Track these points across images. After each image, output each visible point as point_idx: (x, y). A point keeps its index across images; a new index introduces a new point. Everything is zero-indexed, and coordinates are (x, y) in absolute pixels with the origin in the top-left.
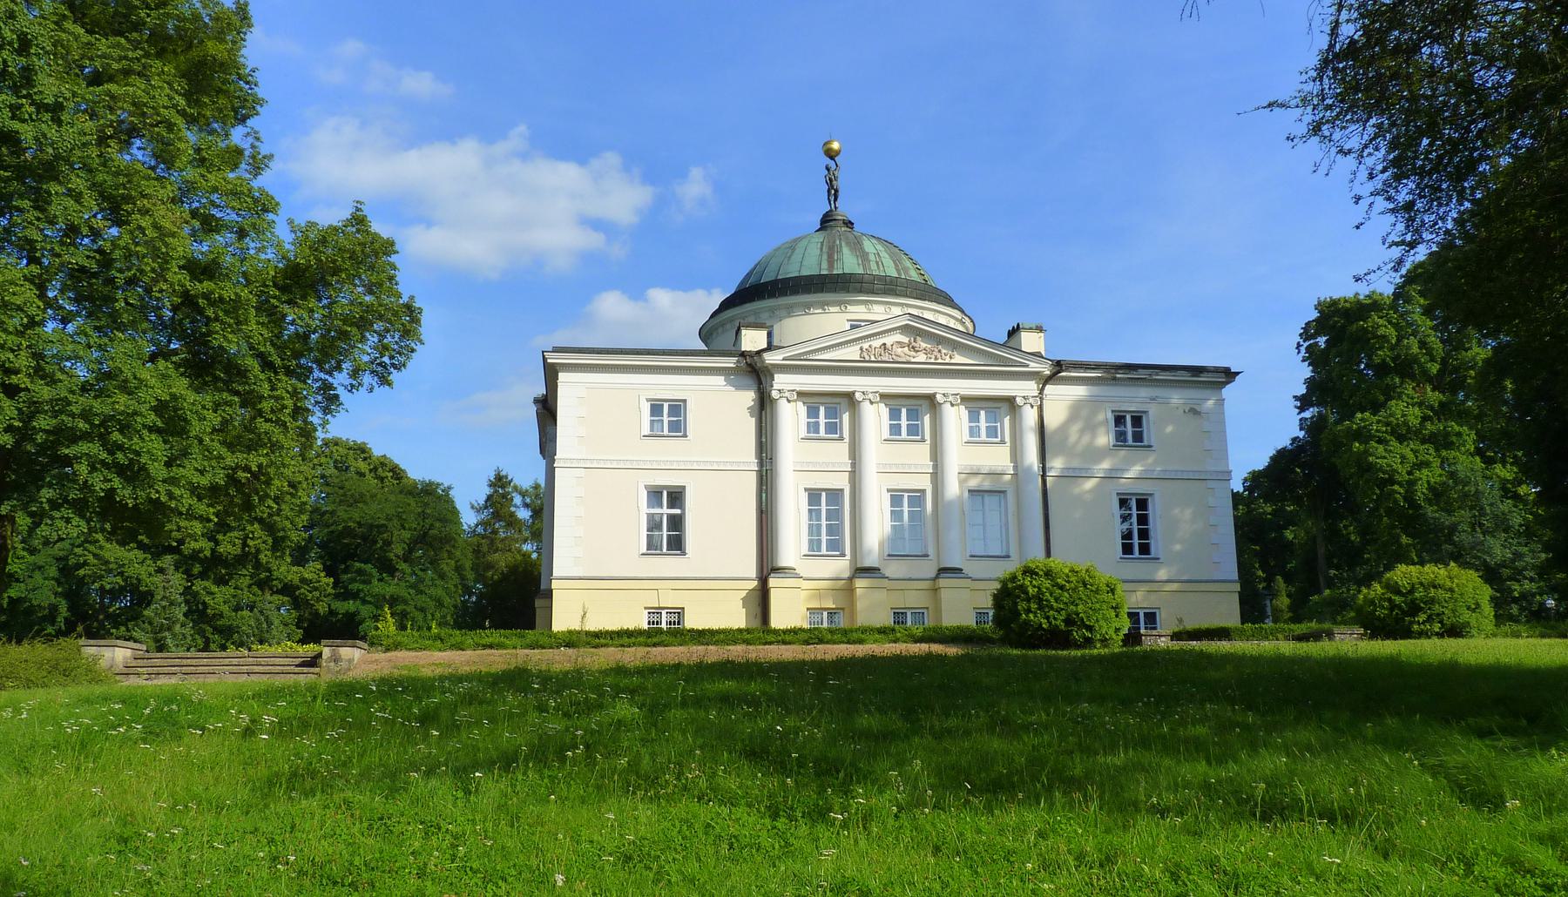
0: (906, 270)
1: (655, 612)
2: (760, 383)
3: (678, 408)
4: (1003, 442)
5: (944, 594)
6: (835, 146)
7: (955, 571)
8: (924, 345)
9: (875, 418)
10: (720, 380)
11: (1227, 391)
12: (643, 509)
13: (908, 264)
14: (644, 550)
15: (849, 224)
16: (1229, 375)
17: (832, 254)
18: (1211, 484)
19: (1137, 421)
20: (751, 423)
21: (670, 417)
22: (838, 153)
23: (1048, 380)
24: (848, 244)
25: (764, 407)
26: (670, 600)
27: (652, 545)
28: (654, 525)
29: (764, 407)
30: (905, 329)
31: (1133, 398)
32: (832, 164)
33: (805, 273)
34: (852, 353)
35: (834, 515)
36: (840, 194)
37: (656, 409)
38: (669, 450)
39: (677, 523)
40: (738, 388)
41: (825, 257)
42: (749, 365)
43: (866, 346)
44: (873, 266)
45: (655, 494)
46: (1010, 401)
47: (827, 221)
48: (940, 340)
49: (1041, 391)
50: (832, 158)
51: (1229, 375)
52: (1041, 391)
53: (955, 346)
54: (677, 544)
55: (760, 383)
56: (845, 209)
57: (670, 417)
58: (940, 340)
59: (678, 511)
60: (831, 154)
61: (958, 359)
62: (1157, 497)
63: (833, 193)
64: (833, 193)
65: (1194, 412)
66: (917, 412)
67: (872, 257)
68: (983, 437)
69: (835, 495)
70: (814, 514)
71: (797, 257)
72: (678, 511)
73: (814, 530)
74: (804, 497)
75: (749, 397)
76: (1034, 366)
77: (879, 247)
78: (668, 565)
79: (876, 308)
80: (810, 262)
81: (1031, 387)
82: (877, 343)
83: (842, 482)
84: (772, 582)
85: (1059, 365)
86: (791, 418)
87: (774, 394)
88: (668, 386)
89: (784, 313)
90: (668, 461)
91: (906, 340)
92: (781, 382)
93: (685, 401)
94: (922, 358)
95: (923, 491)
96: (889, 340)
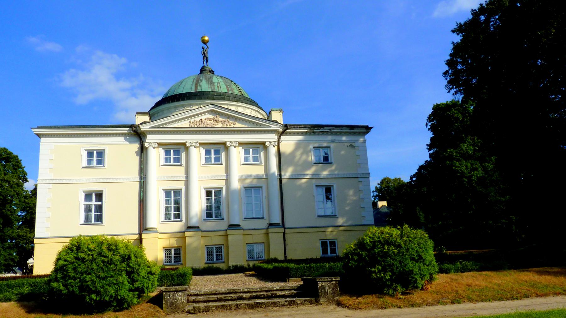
0: (232, 90)
2: (141, 139)
3: (100, 154)
4: (261, 163)
5: (230, 238)
6: (206, 38)
7: (237, 226)
8: (221, 119)
9: (197, 155)
10: (122, 139)
11: (367, 136)
12: (82, 203)
13: (234, 87)
14: (82, 222)
15: (212, 72)
16: (368, 129)
17: (197, 82)
18: (360, 180)
20: (137, 159)
22: (208, 41)
23: (283, 133)
24: (206, 79)
25: (143, 150)
27: (87, 219)
28: (88, 209)
29: (143, 150)
30: (211, 112)
31: (325, 140)
32: (205, 46)
33: (184, 92)
35: (177, 202)
36: (209, 59)
37: (90, 154)
39: (99, 208)
40: (131, 142)
41: (194, 85)
42: (135, 131)
43: (192, 120)
44: (216, 88)
45: (88, 196)
46: (263, 144)
47: (202, 70)
48: (229, 117)
49: (279, 138)
50: (205, 44)
51: (368, 129)
52: (279, 138)
53: (236, 119)
54: (99, 219)
55: (141, 139)
56: (210, 66)
57: (97, 157)
58: (229, 117)
59: (100, 203)
60: (205, 42)
61: (238, 125)
62: (335, 186)
63: (205, 58)
64: (205, 58)
65: (352, 146)
66: (216, 151)
67: (216, 84)
68: (251, 161)
69: (177, 192)
70: (167, 201)
71: (182, 86)
72: (100, 203)
73: (167, 209)
74: (163, 194)
75: (136, 147)
76: (274, 127)
77: (221, 80)
80: (188, 88)
81: (274, 137)
82: (198, 119)
83: (181, 185)
84: (143, 236)
86: (156, 156)
87: (146, 145)
88: (95, 143)
89: (173, 110)
90: (95, 179)
91: (212, 117)
92: (150, 139)
93: (104, 150)
95: (222, 188)
96: (203, 117)
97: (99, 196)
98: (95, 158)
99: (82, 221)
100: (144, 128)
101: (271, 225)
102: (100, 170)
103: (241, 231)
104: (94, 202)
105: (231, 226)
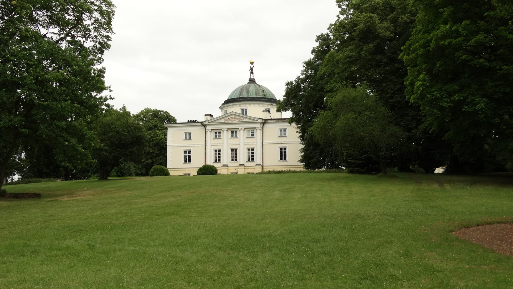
1: (185, 175)
3: (190, 134)
5: (239, 170)
12: (183, 154)
19: (285, 130)
21: (188, 136)
26: (187, 172)
28: (185, 157)
34: (222, 121)
37: (186, 134)
39: (190, 157)
45: (186, 152)
54: (190, 161)
57: (188, 136)
64: (252, 72)
78: (187, 165)
79: (248, 105)
85: (266, 120)
88: (188, 130)
90: (188, 145)
92: (209, 128)
94: (237, 121)
96: (230, 117)
97: (190, 152)
98: (188, 136)
99: (183, 161)
100: (205, 123)
101: (257, 165)
102: (189, 141)
103: (244, 167)
104: (188, 154)
105: (241, 165)
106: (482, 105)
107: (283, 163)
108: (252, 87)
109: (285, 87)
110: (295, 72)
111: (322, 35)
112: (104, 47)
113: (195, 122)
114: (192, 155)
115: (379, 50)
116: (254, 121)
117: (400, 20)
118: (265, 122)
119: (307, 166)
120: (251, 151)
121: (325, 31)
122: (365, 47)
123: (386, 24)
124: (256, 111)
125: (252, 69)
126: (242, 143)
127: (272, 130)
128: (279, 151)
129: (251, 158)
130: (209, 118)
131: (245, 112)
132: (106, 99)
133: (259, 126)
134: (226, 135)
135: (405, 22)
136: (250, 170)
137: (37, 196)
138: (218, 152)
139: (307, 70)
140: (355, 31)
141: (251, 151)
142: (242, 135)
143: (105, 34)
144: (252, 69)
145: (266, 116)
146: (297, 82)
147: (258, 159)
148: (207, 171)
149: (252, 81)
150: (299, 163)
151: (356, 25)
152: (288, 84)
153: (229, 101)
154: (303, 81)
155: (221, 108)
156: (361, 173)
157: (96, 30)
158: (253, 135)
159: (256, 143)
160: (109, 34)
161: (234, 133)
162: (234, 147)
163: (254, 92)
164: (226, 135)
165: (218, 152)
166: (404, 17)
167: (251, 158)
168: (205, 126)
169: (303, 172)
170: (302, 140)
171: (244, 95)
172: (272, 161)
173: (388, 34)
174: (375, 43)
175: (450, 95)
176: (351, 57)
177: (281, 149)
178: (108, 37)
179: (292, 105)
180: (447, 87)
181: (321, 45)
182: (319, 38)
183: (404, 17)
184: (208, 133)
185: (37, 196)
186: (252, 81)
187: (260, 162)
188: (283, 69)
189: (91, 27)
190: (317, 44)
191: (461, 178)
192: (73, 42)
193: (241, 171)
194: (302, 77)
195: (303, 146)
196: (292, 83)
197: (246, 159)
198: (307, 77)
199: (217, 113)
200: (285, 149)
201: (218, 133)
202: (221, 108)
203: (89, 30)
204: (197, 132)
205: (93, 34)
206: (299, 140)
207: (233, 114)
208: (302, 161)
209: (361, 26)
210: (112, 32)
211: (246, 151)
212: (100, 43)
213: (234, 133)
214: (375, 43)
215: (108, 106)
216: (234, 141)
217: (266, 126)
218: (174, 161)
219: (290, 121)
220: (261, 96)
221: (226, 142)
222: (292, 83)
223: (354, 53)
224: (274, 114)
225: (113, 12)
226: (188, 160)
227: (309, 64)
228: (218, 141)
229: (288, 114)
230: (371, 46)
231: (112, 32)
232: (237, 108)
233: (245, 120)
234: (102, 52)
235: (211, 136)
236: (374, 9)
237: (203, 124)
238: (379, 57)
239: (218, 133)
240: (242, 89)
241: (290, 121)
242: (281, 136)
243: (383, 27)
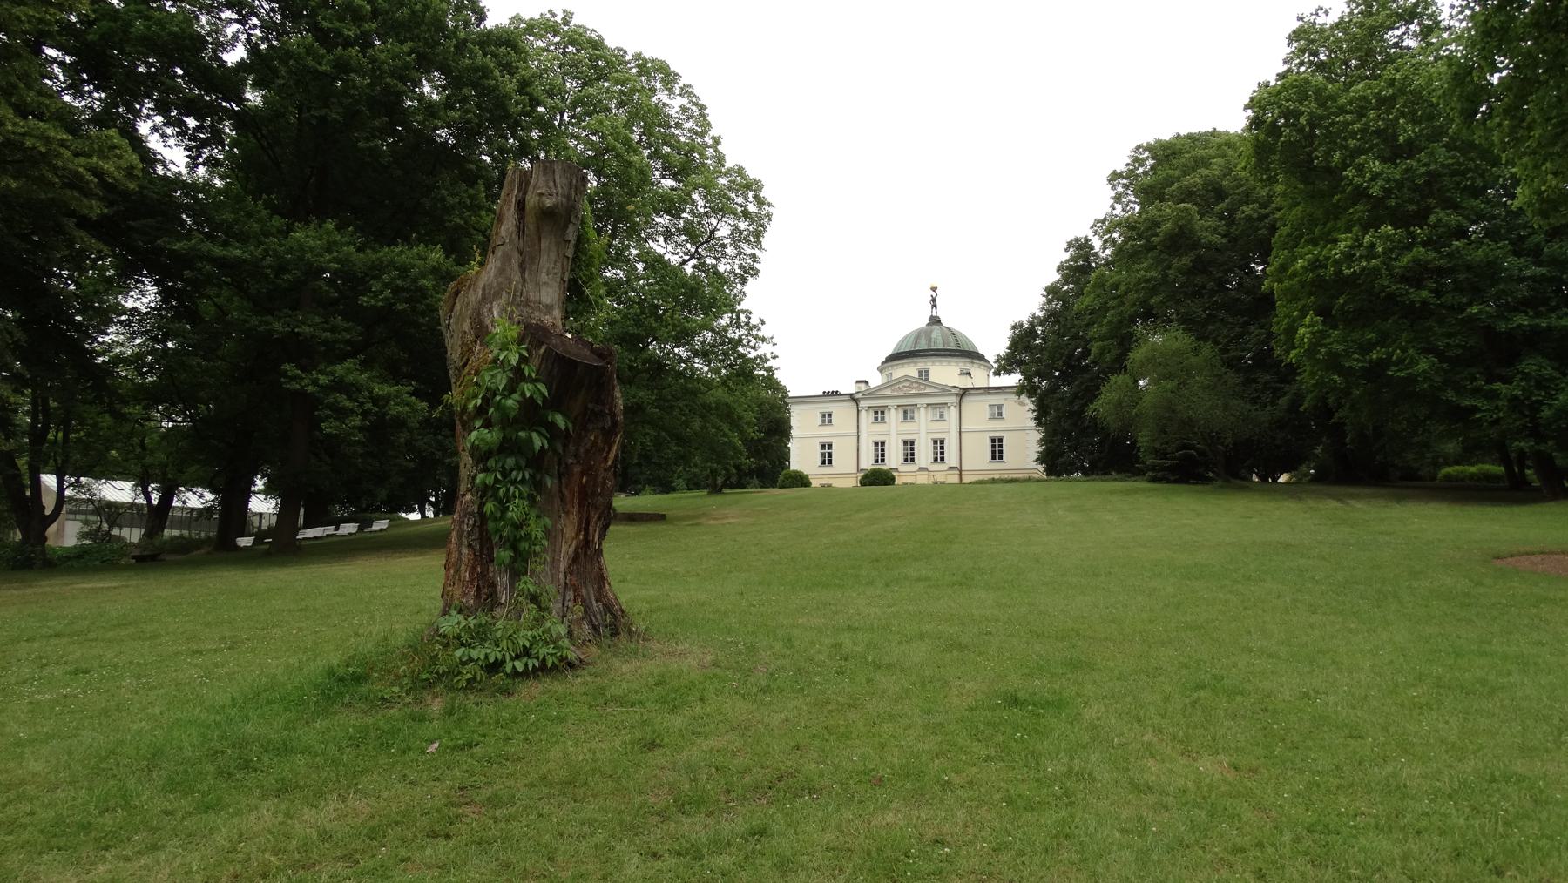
12: (819, 450)
19: (1000, 407)
21: (827, 418)
26: (826, 481)
28: (823, 455)
34: (888, 392)
38: (827, 431)
39: (830, 455)
45: (823, 446)
54: (830, 462)
57: (827, 418)
64: (935, 306)
78: (826, 470)
85: (966, 390)
88: (827, 408)
90: (826, 434)
92: (863, 404)
97: (830, 446)
105: (921, 469)
106: (1423, 365)
107: (997, 465)
108: (936, 332)
109: (1010, 333)
110: (1029, 304)
111: (1077, 240)
112: (748, 273)
113: (835, 394)
114: (834, 451)
115: (1200, 267)
116: (944, 391)
117: (1239, 214)
118: (964, 393)
119: (1049, 471)
120: (939, 445)
121: (1083, 230)
122: (1176, 263)
123: (1210, 222)
124: (946, 374)
125: (934, 300)
126: (924, 429)
127: (977, 410)
128: (989, 444)
129: (940, 456)
130: (863, 387)
131: (924, 374)
132: (763, 359)
133: (953, 400)
134: (893, 417)
135: (1249, 219)
136: (940, 479)
137: (660, 518)
138: (880, 447)
139: (1049, 302)
140: (1156, 235)
141: (939, 445)
142: (922, 416)
143: (749, 251)
144: (934, 300)
145: (966, 383)
146: (1031, 323)
147: (951, 458)
148: (878, 478)
149: (935, 321)
150: (1034, 465)
151: (1156, 224)
152: (1014, 327)
153: (895, 358)
154: (1042, 322)
155: (880, 370)
156: (1169, 481)
157: (735, 244)
158: (942, 415)
159: (948, 429)
160: (756, 252)
161: (908, 413)
162: (908, 437)
163: (940, 341)
164: (893, 417)
165: (880, 447)
166: (1248, 210)
167: (940, 456)
168: (856, 401)
169: (1039, 481)
170: (1039, 424)
171: (923, 345)
172: (978, 461)
173: (1216, 238)
174: (1192, 255)
175: (1365, 348)
176: (1147, 281)
177: (993, 441)
178: (753, 256)
179: (1020, 363)
180: (1355, 336)
181: (1073, 258)
182: (1070, 244)
183: (1248, 210)
184: (863, 413)
185: (660, 518)
186: (935, 321)
187: (955, 463)
188: (1001, 296)
189: (727, 241)
190: (1067, 256)
191: (1367, 491)
192: (702, 266)
193: (922, 479)
194: (1041, 314)
195: (1040, 436)
196: (1021, 325)
197: (931, 457)
198: (1051, 314)
199: (876, 380)
200: (1001, 440)
201: (879, 414)
202: (880, 370)
203: (724, 246)
204: (843, 414)
205: (730, 250)
206: (1033, 424)
207: (906, 379)
208: (1040, 460)
209: (1166, 227)
210: (761, 249)
211: (931, 444)
212: (741, 267)
213: (908, 413)
214: (1192, 255)
215: (769, 369)
216: (908, 427)
217: (965, 399)
218: (801, 457)
219: (1020, 390)
220: (953, 346)
221: (894, 430)
222: (1021, 325)
223: (1154, 274)
224: (981, 377)
225: (769, 216)
226: (827, 460)
227: (1052, 291)
228: (879, 428)
229: (1014, 379)
230: (1186, 260)
231: (761, 249)
232: (910, 370)
233: (928, 390)
234: (744, 281)
235: (867, 418)
236: (1188, 195)
237: (853, 398)
238: (1200, 280)
239: (879, 414)
240: (919, 334)
241: (1020, 390)
242: (993, 418)
243: (1207, 228)
